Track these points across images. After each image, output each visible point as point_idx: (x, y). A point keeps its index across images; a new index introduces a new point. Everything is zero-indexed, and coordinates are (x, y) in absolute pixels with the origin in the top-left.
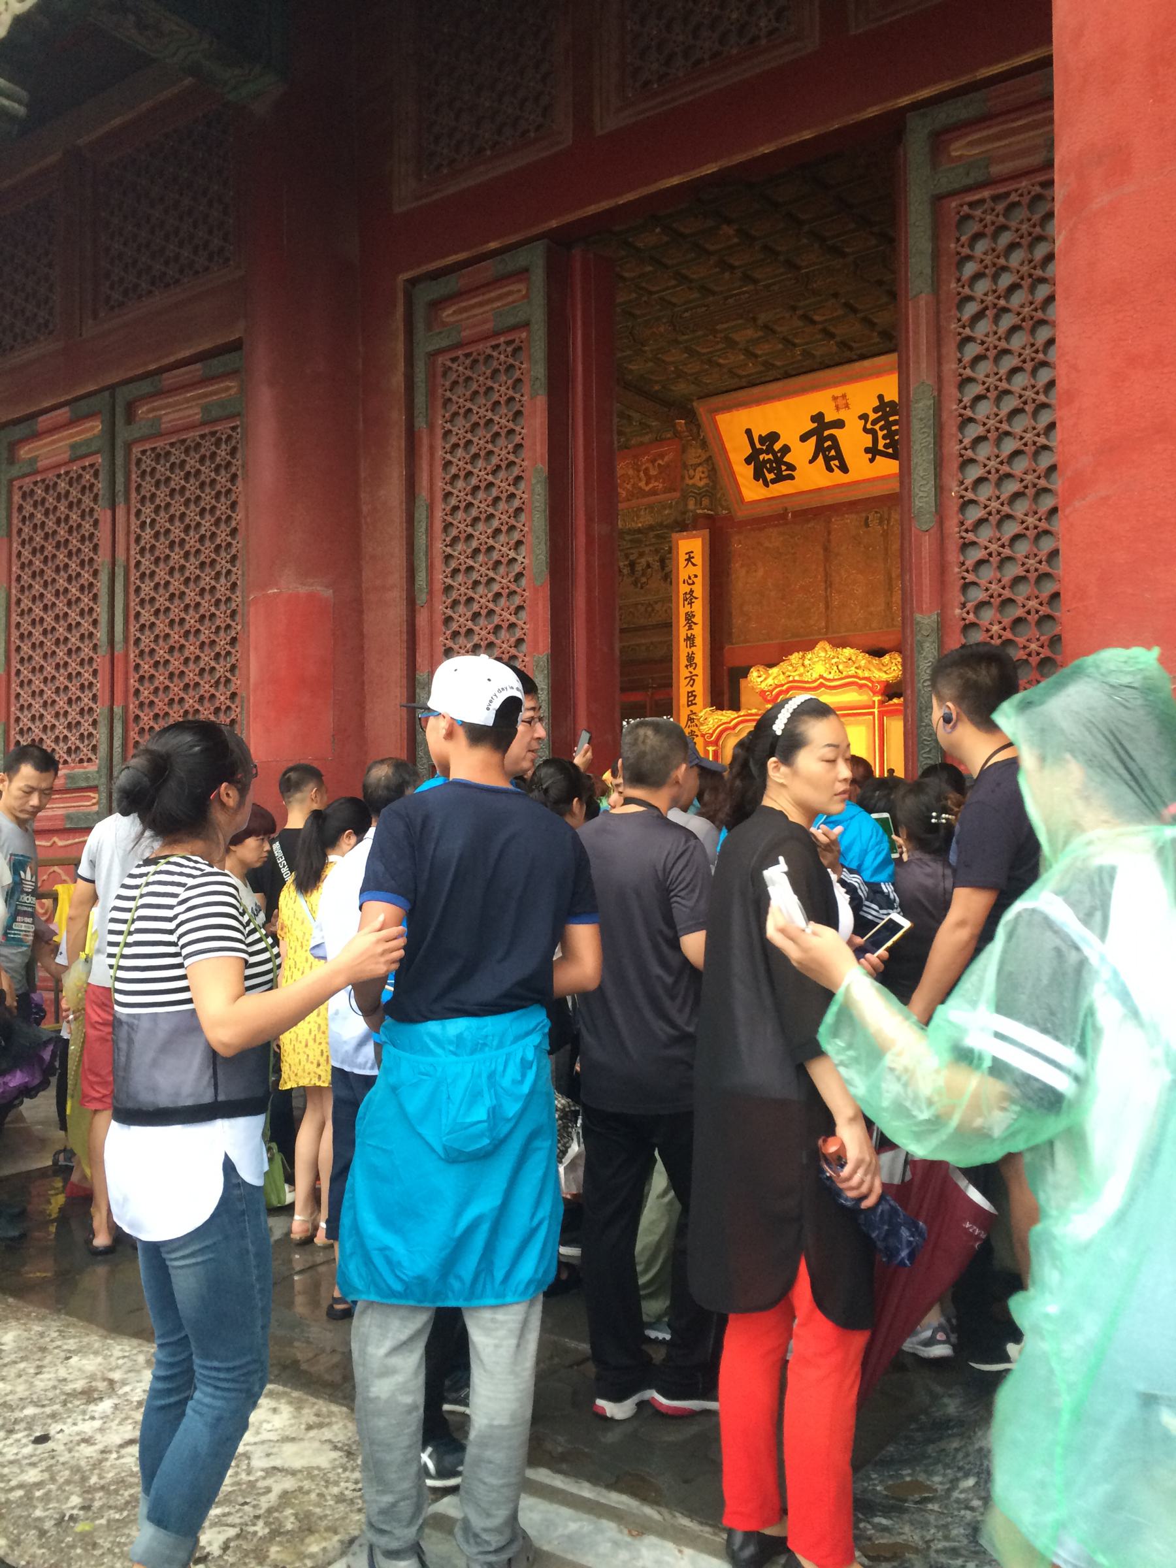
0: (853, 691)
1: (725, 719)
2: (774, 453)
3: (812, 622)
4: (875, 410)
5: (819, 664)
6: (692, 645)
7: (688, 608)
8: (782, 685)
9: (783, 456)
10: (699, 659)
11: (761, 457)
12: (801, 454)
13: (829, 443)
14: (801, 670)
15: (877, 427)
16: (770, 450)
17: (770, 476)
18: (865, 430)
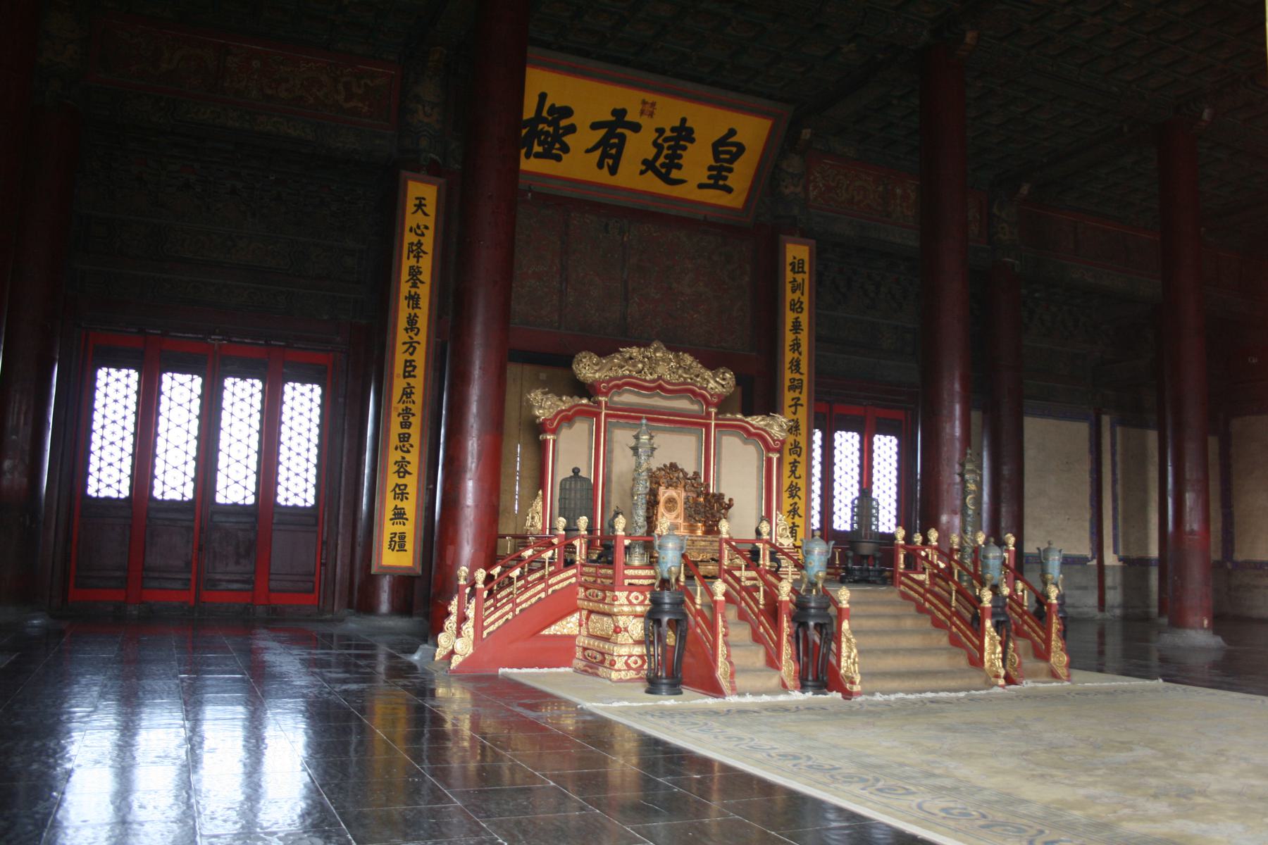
0: (687, 398)
2: (557, 128)
4: (673, 129)
6: (416, 306)
7: (413, 261)
10: (422, 323)
11: (541, 126)
12: (583, 139)
13: (616, 141)
14: (640, 366)
15: (666, 145)
16: (555, 123)
17: (537, 149)
18: (655, 144)
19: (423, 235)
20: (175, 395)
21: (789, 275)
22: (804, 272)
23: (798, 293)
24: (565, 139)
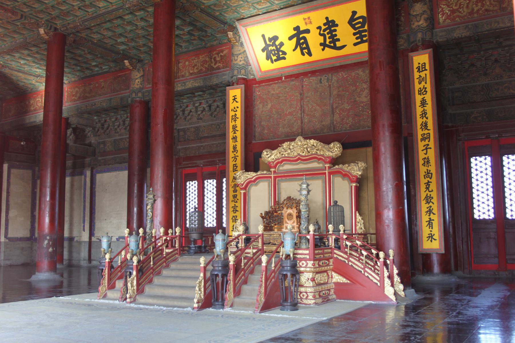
1: (249, 177)
2: (276, 46)
3: (294, 130)
4: (325, 25)
5: (298, 147)
7: (233, 123)
8: (279, 159)
9: (280, 47)
10: (239, 148)
11: (270, 48)
12: (289, 46)
13: (302, 41)
14: (289, 151)
15: (326, 33)
16: (274, 44)
17: (274, 58)
18: (320, 34)
19: (236, 111)
20: (209, 187)
21: (416, 75)
22: (427, 70)
23: (423, 83)
24: (282, 49)
